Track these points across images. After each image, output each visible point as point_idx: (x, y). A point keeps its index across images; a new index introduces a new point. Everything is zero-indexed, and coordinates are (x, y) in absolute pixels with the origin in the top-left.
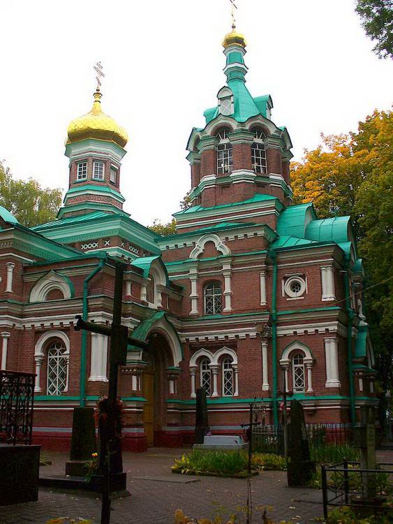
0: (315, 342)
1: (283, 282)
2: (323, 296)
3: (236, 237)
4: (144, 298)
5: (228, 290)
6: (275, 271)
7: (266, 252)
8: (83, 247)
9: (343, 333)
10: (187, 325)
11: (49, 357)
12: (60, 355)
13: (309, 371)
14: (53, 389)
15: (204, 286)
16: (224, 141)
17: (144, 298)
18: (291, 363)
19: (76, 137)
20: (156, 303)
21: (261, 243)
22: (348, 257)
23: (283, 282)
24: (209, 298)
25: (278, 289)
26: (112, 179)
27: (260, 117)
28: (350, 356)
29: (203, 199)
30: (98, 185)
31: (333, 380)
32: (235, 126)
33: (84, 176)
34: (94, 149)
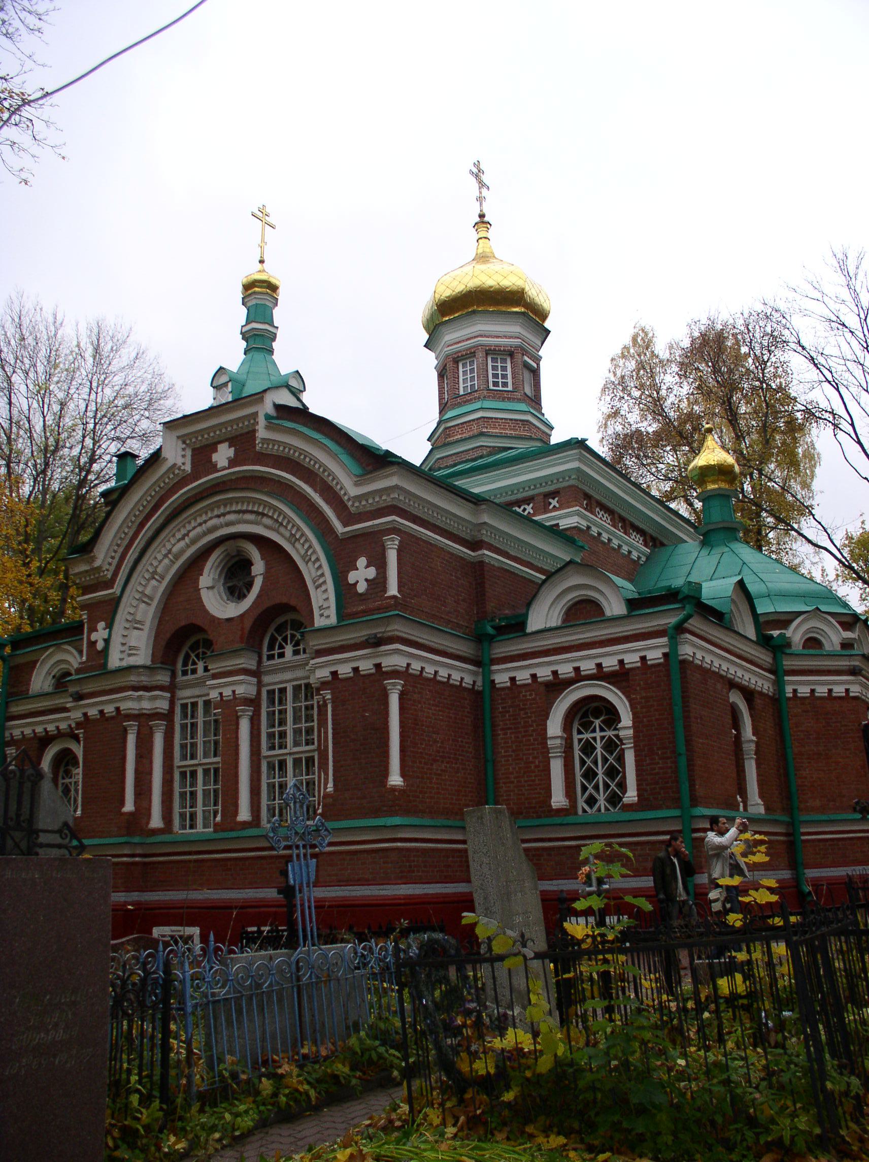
19: (450, 310)
26: (528, 390)
34: (487, 332)
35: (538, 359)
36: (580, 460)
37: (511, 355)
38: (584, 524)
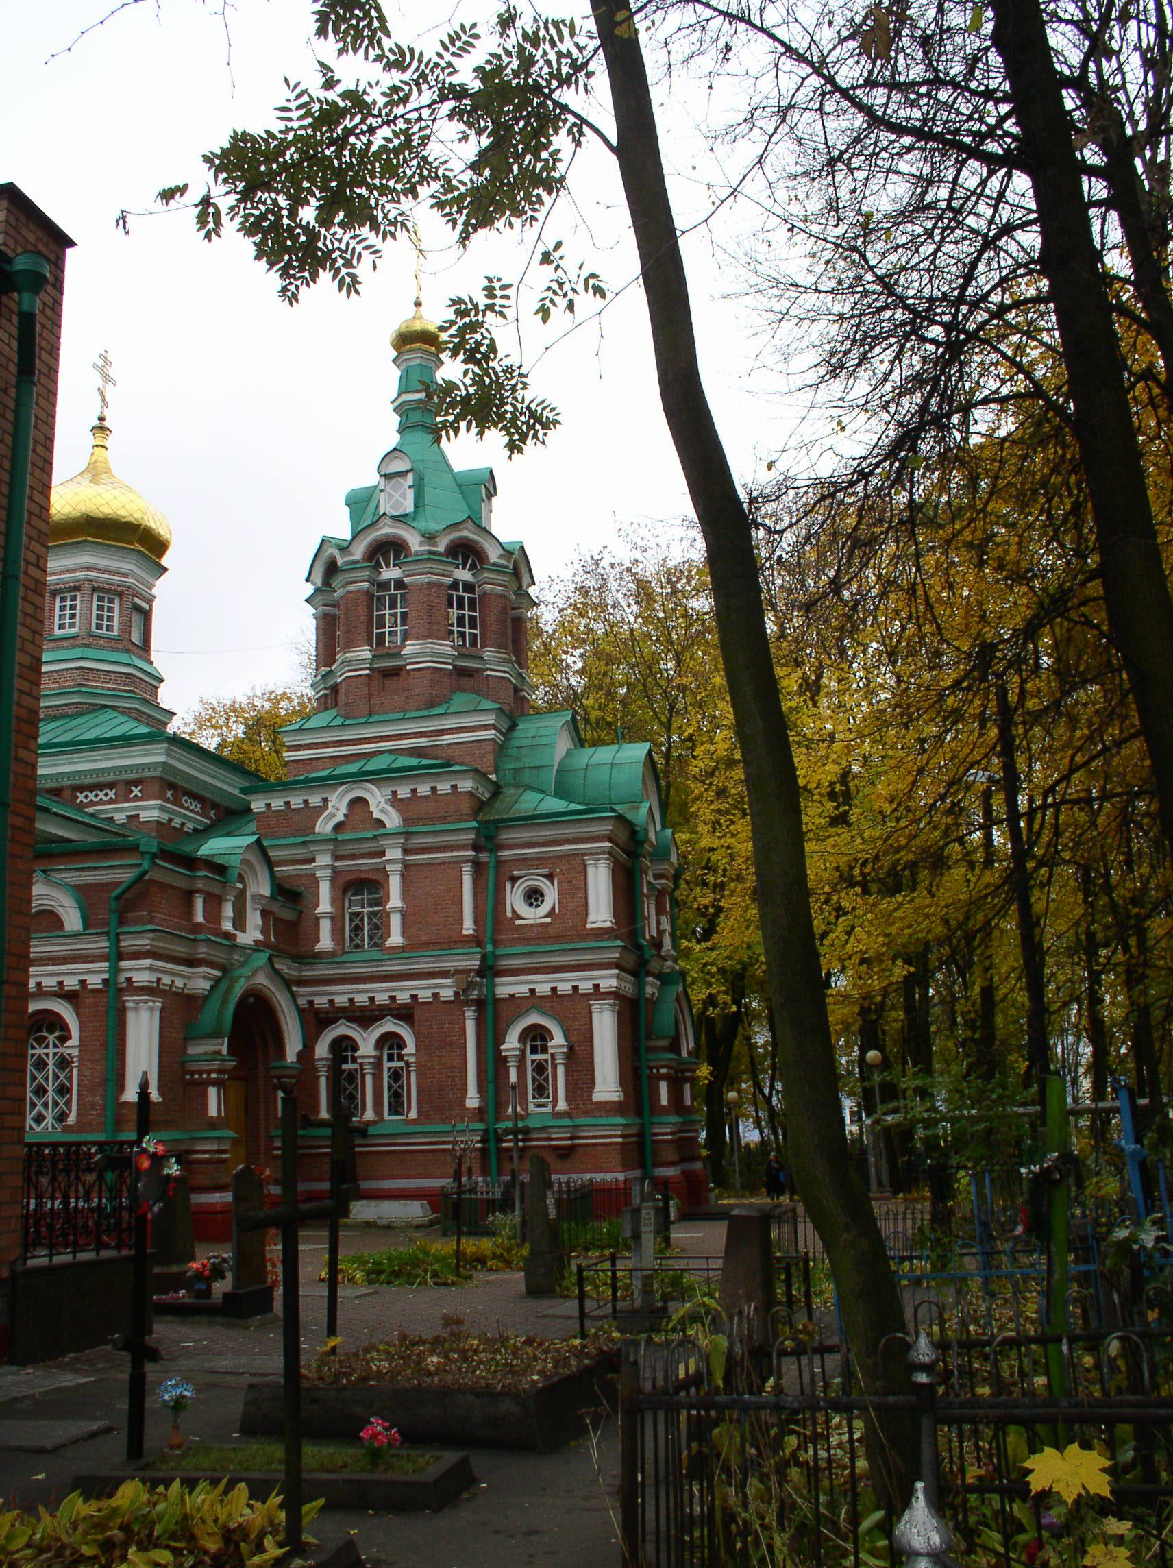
0: (572, 1012)
1: (508, 885)
2: (591, 918)
3: (414, 791)
4: (227, 926)
5: (395, 900)
6: (492, 864)
7: (474, 824)
8: (81, 797)
9: (628, 989)
10: (308, 973)
11: (31, 1052)
12: (55, 1046)
13: (561, 1071)
14: (39, 1119)
15: (345, 891)
16: (390, 573)
17: (227, 926)
18: (523, 1051)
20: (251, 934)
21: (466, 806)
22: (641, 836)
23: (508, 885)
25: (499, 902)
26: (136, 637)
27: (470, 524)
28: (643, 1036)
29: (342, 698)
30: (105, 648)
31: (607, 1084)
32: (415, 543)
33: (72, 625)
35: (150, 600)
36: (168, 755)
37: (120, 595)
38: (165, 817)
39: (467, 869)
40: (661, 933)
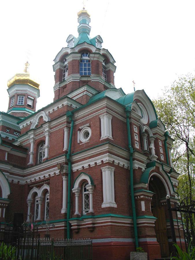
23: (78, 132)
24: (41, 153)
27: (86, 44)
39: (65, 129)
40: (150, 149)
